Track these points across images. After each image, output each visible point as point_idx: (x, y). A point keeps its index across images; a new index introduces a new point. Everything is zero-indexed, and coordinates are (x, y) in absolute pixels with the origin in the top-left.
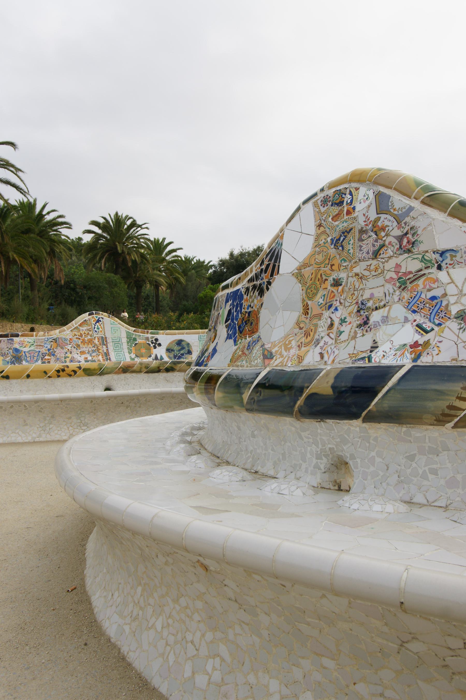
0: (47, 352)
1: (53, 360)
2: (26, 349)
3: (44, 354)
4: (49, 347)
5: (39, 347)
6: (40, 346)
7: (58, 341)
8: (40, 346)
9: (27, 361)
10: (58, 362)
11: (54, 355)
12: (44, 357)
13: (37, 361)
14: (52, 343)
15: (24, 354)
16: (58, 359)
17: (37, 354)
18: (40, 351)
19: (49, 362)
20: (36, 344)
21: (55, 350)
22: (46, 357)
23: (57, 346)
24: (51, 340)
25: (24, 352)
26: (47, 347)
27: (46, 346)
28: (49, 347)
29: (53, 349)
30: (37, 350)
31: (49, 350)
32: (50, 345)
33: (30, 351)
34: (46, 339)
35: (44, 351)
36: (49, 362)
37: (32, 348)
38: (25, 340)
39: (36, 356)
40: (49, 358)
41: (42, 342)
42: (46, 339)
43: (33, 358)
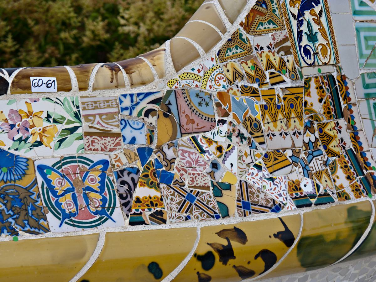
0: (138, 164)
1: (175, 207)
2: (46, 155)
3: (126, 178)
4: (142, 140)
5: (99, 143)
6: (105, 134)
7: (173, 108)
8: (105, 134)
9: (65, 217)
10: (196, 212)
11: (167, 178)
12: (130, 192)
13: (105, 213)
14: (152, 119)
15: (40, 180)
16: (190, 198)
17: (96, 175)
18: (105, 163)
19: (159, 217)
20: (85, 127)
21: (170, 154)
22: (141, 192)
23: (174, 137)
24: (144, 105)
25: (41, 168)
26: (133, 141)
27: (128, 133)
28: (142, 140)
29: (160, 149)
30: (96, 157)
31: (143, 153)
32: (145, 131)
33: (64, 161)
34: (127, 103)
35: (124, 160)
36: (159, 217)
37: (72, 147)
38: (36, 108)
39: (96, 186)
40: (153, 193)
41: (111, 116)
42: (127, 103)
43: (86, 197)
